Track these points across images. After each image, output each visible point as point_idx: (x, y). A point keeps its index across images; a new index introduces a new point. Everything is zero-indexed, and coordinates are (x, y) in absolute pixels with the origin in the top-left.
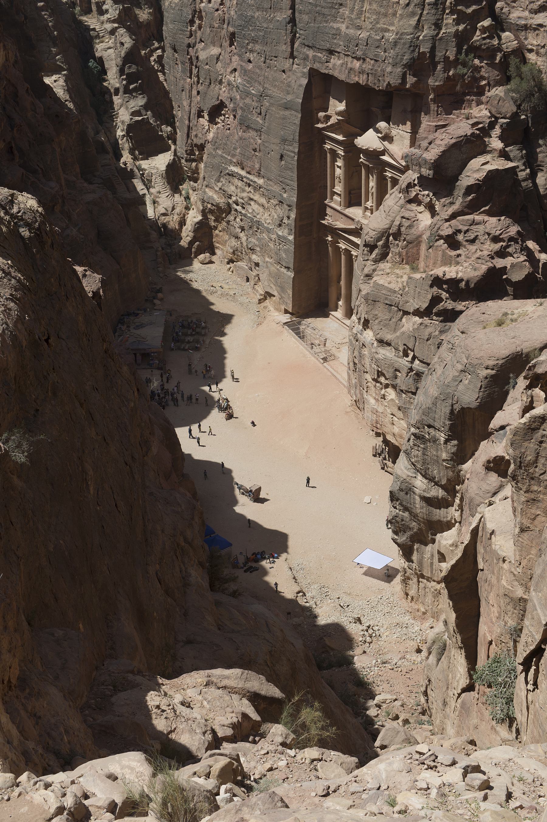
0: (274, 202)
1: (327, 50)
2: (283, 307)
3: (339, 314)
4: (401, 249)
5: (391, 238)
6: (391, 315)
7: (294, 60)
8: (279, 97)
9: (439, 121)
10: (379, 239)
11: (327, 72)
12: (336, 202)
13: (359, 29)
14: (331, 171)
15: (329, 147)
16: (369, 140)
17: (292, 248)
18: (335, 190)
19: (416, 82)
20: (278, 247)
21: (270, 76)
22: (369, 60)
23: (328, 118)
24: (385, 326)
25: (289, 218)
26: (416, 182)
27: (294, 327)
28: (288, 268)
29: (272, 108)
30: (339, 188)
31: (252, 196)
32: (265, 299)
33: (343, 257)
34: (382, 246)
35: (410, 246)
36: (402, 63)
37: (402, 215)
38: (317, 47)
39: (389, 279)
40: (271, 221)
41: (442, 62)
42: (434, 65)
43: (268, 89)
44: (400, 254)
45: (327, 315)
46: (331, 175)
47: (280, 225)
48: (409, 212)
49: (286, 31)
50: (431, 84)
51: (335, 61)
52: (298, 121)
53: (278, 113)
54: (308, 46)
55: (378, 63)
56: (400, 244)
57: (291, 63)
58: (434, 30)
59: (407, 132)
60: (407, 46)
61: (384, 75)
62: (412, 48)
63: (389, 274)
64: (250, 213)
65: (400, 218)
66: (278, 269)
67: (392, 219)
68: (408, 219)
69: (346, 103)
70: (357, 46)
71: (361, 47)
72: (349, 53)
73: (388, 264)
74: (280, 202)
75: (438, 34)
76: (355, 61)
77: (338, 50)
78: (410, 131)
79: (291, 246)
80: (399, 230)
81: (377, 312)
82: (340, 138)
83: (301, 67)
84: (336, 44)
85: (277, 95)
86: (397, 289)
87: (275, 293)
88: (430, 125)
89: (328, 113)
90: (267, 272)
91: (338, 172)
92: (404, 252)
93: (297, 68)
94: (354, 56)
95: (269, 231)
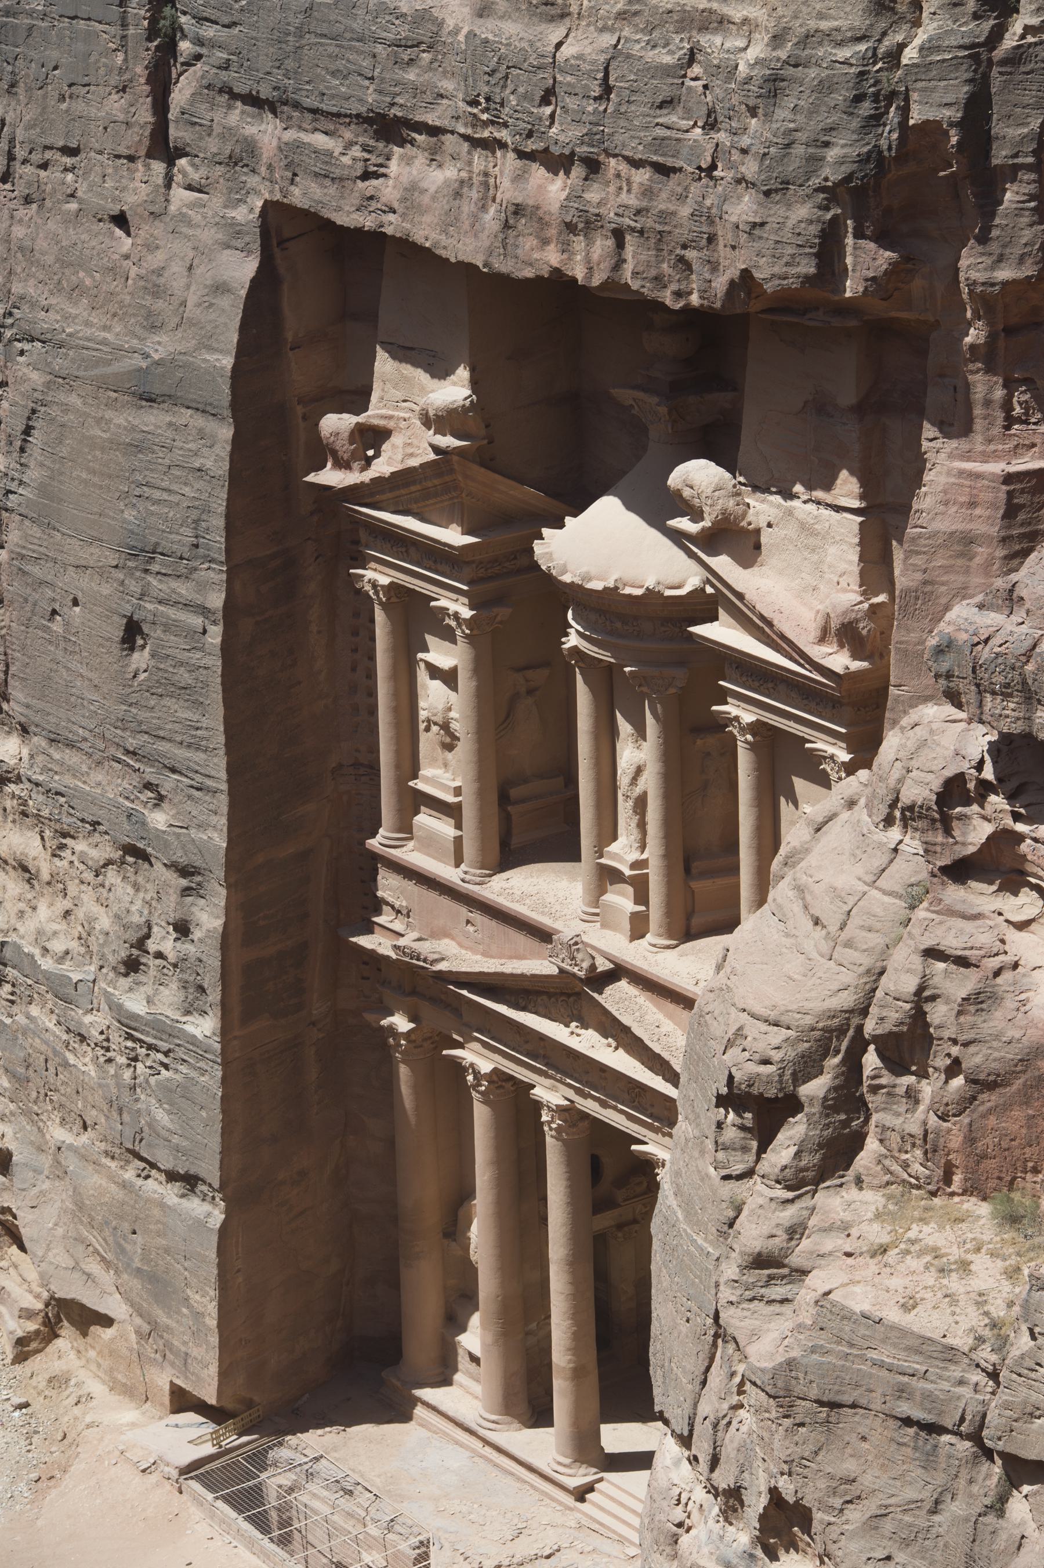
0: (94, 853)
2: (162, 1379)
3: (466, 1397)
4: (933, 1120)
5: (871, 1060)
6: (940, 1479)
7: (171, 163)
8: (104, 342)
9: (1017, 450)
10: (807, 1067)
11: (369, 222)
12: (431, 843)
13: (552, 19)
14: (395, 695)
15: (384, 580)
16: (602, 545)
17: (210, 1080)
18: (420, 785)
19: (894, 271)
20: (127, 1074)
21: (41, 244)
22: (624, 167)
23: (373, 437)
24: (906, 1543)
25: (183, 929)
26: (988, 773)
27: (231, 1482)
28: (190, 1181)
29: (62, 397)
30: (443, 775)
32: (49, 1332)
33: (481, 1114)
34: (821, 1098)
35: (989, 1100)
36: (815, 181)
37: (928, 942)
38: (307, 102)
39: (896, 1282)
40: (74, 945)
41: (1028, 168)
42: (988, 184)
43: (33, 305)
44: (929, 1143)
45: (398, 1410)
46: (396, 710)
47: (132, 966)
48: (960, 923)
49: (124, 25)
50: (974, 275)
52: (217, 458)
53: (99, 421)
54: (253, 100)
55: (673, 183)
56: (927, 1090)
57: (160, 181)
58: (976, 16)
59: (838, 509)
60: (840, 97)
61: (711, 239)
62: (866, 108)
63: (884, 1250)
65: (917, 961)
66: (124, 1185)
67: (867, 961)
68: (963, 962)
69: (473, 371)
70: (545, 101)
71: (572, 103)
72: (503, 135)
73: (868, 1195)
74: (131, 850)
75: (997, 35)
76: (538, 173)
77: (431, 118)
78: (856, 504)
79: (203, 1072)
80: (919, 1017)
81: (849, 1466)
82: (453, 536)
83: (215, 202)
84: (416, 91)
85: (88, 332)
86: (961, 1341)
87: (114, 1306)
88: (978, 476)
89: (375, 413)
90: (60, 1198)
91: (433, 696)
92: (954, 1133)
93: (192, 205)
94: (531, 146)
95: (64, 993)
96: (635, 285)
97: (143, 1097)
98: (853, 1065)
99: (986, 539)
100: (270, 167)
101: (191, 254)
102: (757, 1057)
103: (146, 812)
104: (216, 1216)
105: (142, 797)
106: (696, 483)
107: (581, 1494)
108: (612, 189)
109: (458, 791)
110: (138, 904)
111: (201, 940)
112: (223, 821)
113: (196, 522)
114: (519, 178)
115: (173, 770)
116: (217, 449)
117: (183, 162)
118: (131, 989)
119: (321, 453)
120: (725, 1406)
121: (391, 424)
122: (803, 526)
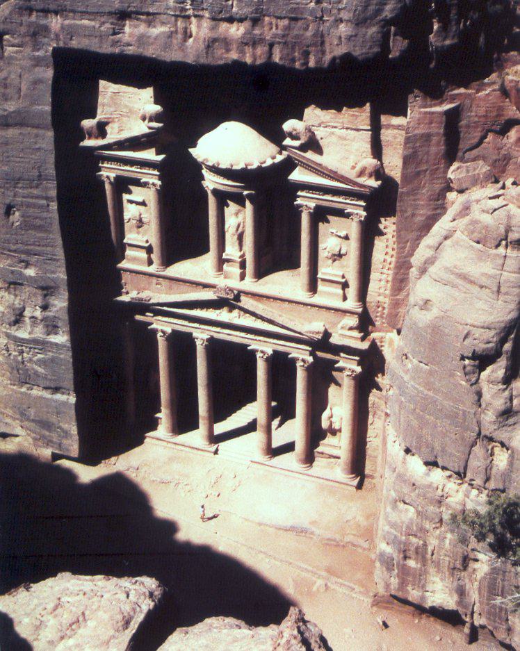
1: (115, 13)
11: (117, 51)
17: (67, 356)
20: (20, 358)
22: (274, 21)
28: (56, 390)
51: (131, 30)
55: (300, 23)
87: (18, 431)
88: (433, 113)
93: (16, 52)
96: (281, 63)
97: (28, 364)
99: (438, 134)
101: (20, 71)
103: (22, 270)
104: (72, 399)
105: (19, 265)
106: (298, 128)
108: (266, 28)
109: (147, 242)
112: (64, 269)
113: (39, 168)
114: (213, 28)
115: (36, 255)
116: (47, 140)
118: (17, 330)
119: (81, 134)
121: (110, 120)
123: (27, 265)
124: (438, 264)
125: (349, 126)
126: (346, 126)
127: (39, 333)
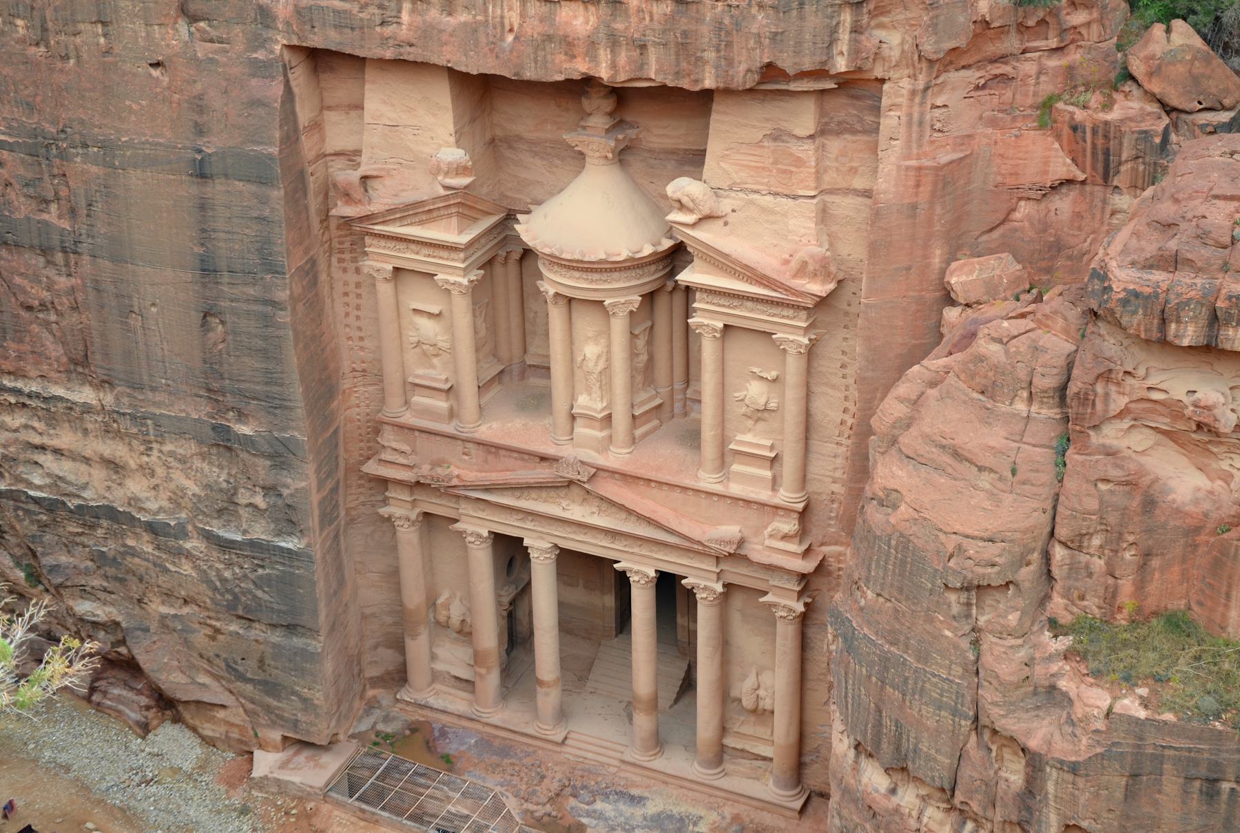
2: (276, 735)
31: (37, 440)
40: (165, 504)
64: (39, 488)
67: (1047, 492)
89: (364, 170)
98: (1047, 557)
100: (288, 23)
102: (983, 563)
107: (563, 742)
108: (634, 20)
110: (223, 477)
111: (291, 495)
117: (202, 24)
120: (992, 772)
122: (764, 210)
123: (242, 416)
124: (914, 431)
125: (779, 190)
126: (774, 189)
127: (260, 532)
